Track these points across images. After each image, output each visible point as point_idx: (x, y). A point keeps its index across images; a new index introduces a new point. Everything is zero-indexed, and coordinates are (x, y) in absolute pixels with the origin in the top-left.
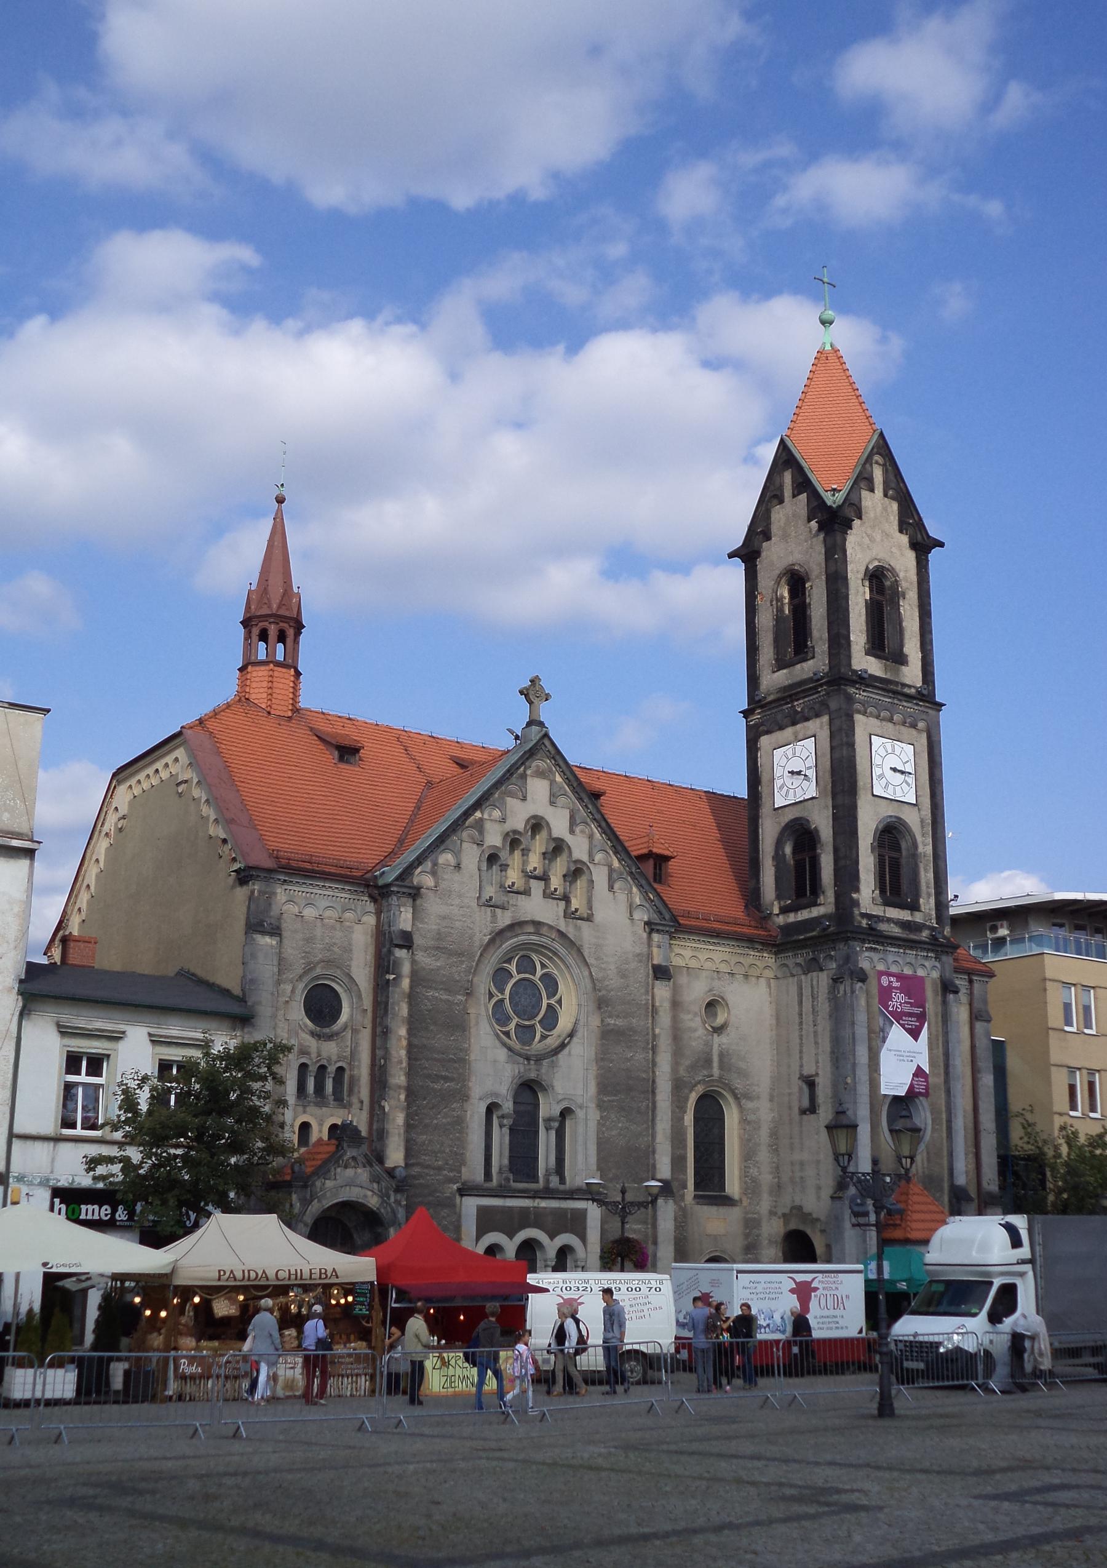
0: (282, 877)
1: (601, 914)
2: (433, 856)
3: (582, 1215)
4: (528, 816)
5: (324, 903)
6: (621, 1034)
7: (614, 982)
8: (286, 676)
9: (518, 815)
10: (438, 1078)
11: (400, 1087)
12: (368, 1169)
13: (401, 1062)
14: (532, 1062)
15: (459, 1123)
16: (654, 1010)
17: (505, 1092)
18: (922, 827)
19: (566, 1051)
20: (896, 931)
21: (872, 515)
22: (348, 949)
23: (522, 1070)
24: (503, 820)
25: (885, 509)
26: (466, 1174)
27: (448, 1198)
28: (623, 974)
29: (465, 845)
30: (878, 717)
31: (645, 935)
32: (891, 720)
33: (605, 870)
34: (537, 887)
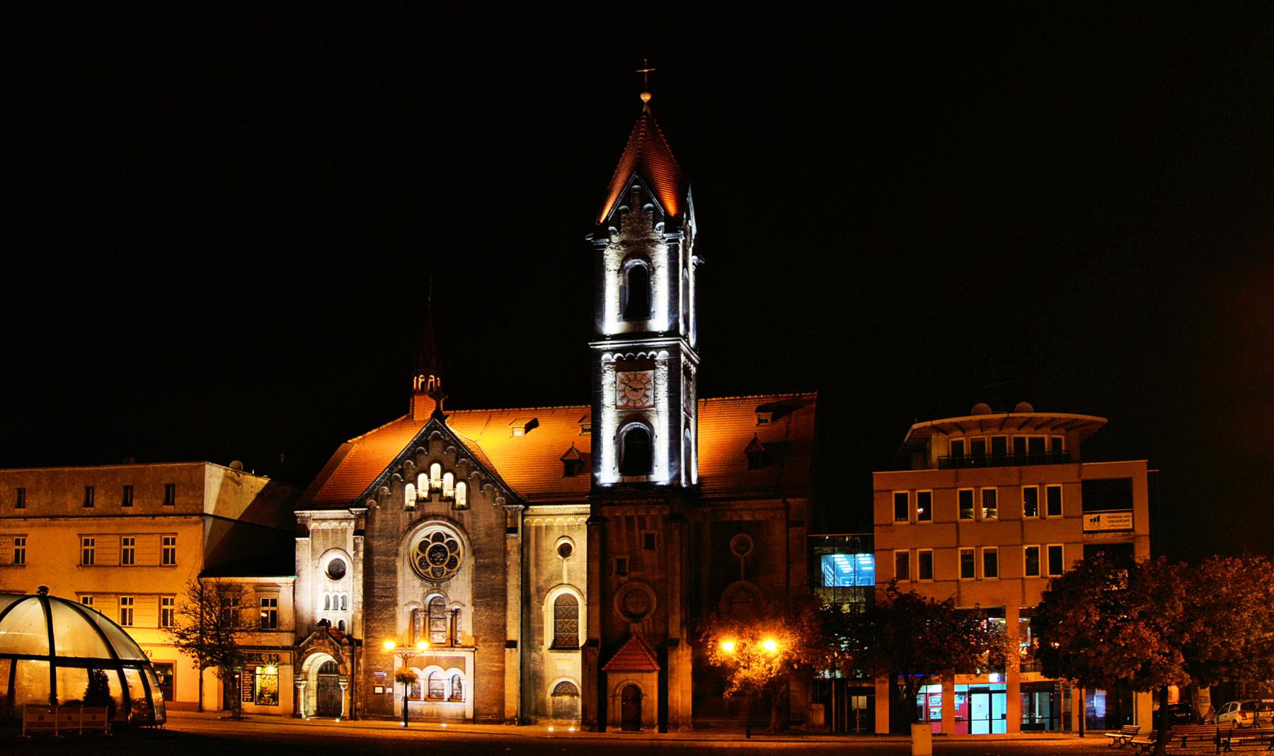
3: (464, 659)
10: (381, 597)
15: (393, 617)
16: (505, 553)
28: (487, 535)
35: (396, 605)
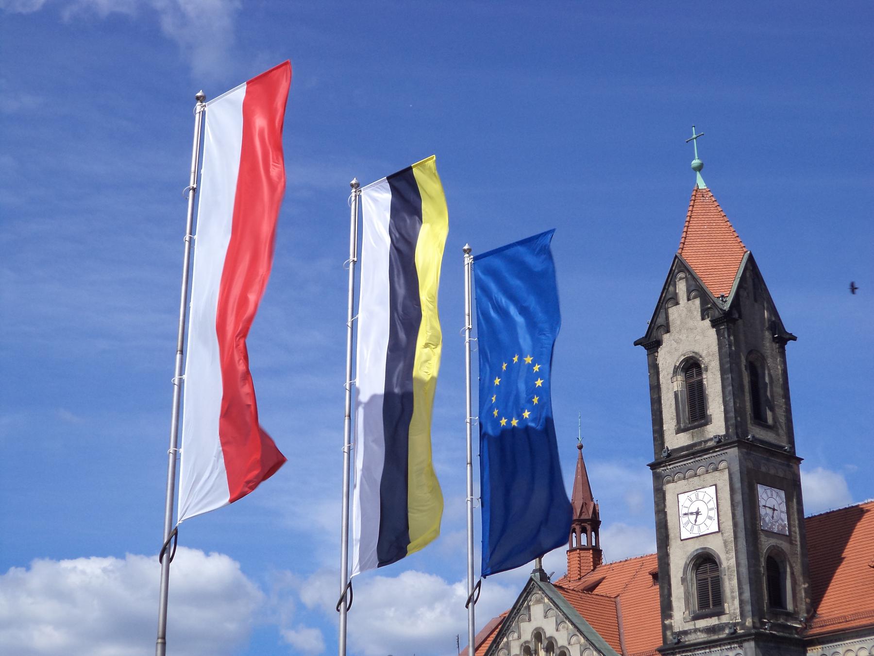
18: (726, 546)
20: (702, 637)
21: (678, 322)
24: (519, 637)
25: (690, 311)
30: (684, 478)
32: (696, 475)
33: (578, 646)
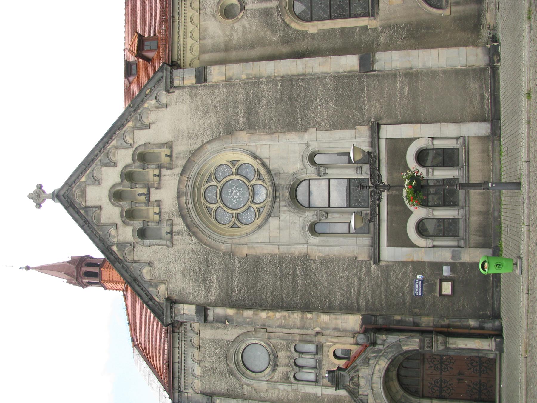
0: (177, 394)
1: (166, 136)
2: (146, 286)
3: (391, 142)
4: (110, 205)
5: (189, 360)
6: (247, 115)
7: (212, 118)
8: (105, 273)
9: (111, 213)
10: (294, 280)
11: (302, 318)
12: (359, 368)
13: (284, 317)
14: (278, 194)
15: (326, 262)
16: (230, 82)
17: (301, 219)
19: (267, 161)
22: (217, 342)
23: (283, 203)
24: (115, 226)
26: (363, 255)
27: (381, 272)
28: (207, 111)
29: (136, 258)
31: (177, 92)
33: (136, 132)
34: (155, 195)
35: (306, 258)
